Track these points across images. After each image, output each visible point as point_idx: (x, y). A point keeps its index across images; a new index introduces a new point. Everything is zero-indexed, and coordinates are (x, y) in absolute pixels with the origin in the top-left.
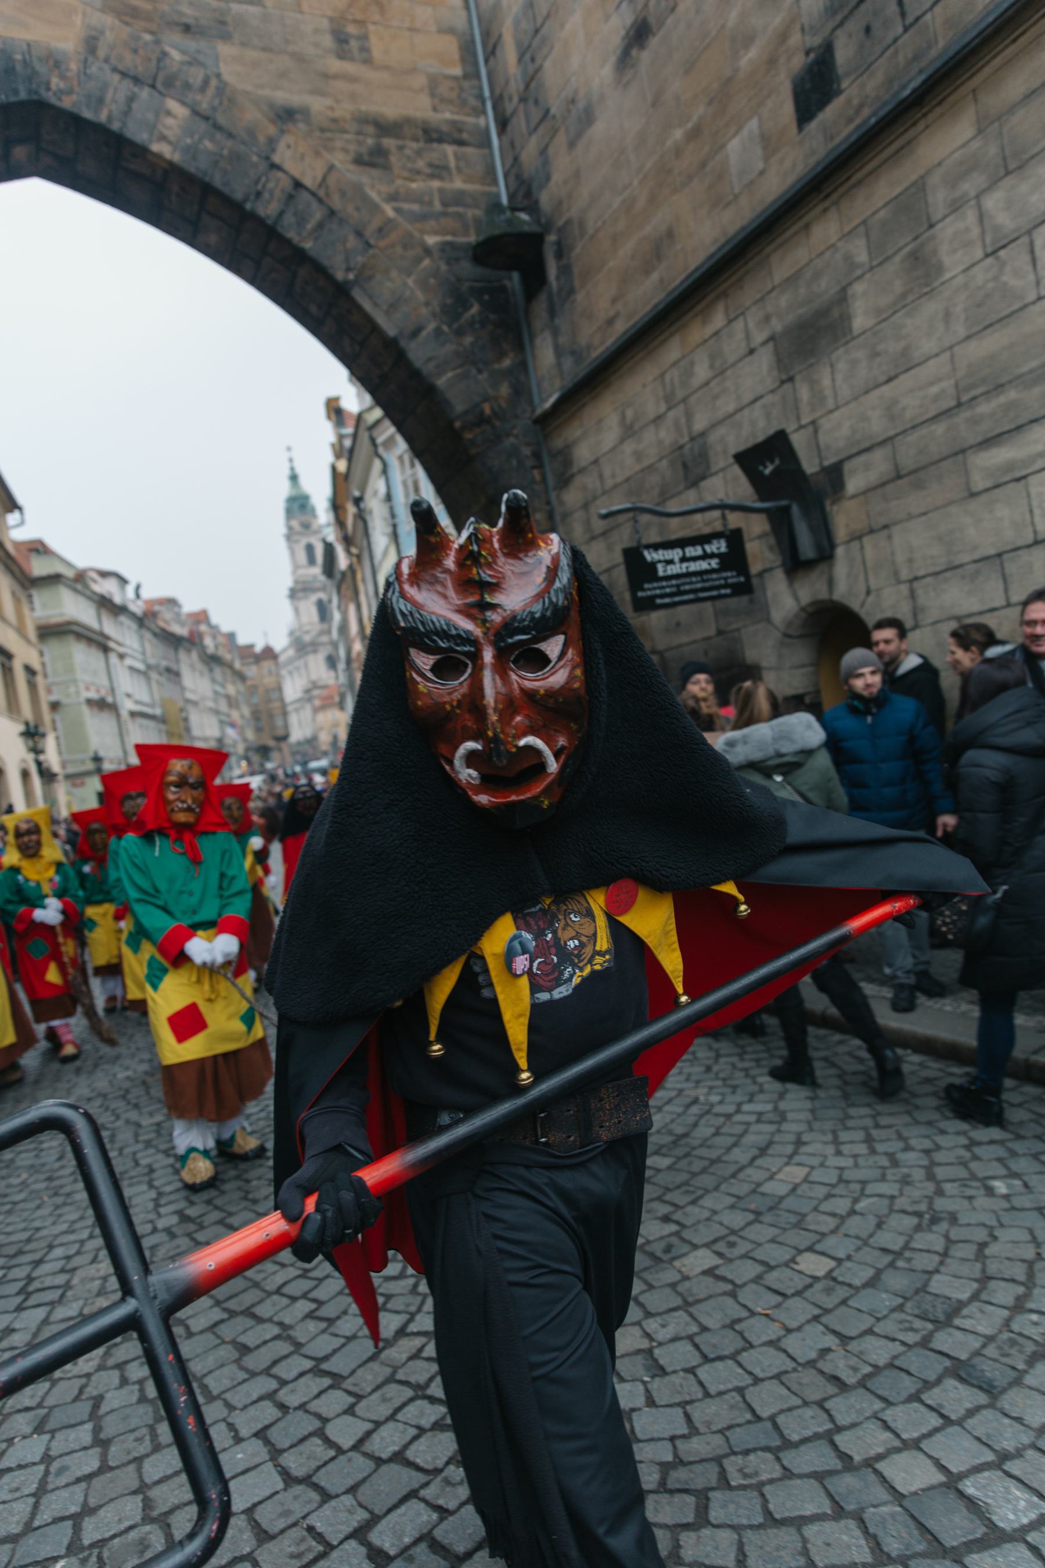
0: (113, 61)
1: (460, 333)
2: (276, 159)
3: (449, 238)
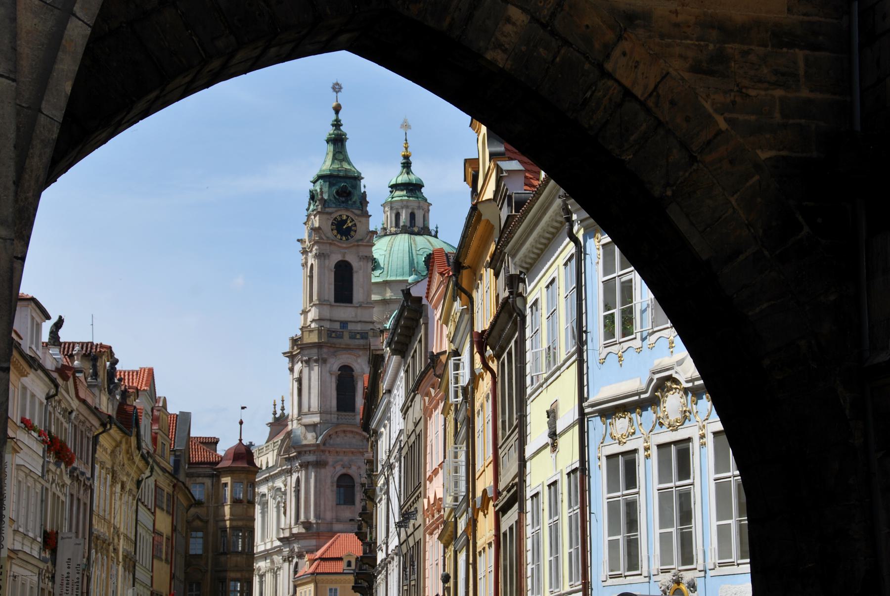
2: (609, 67)
3: (784, 153)
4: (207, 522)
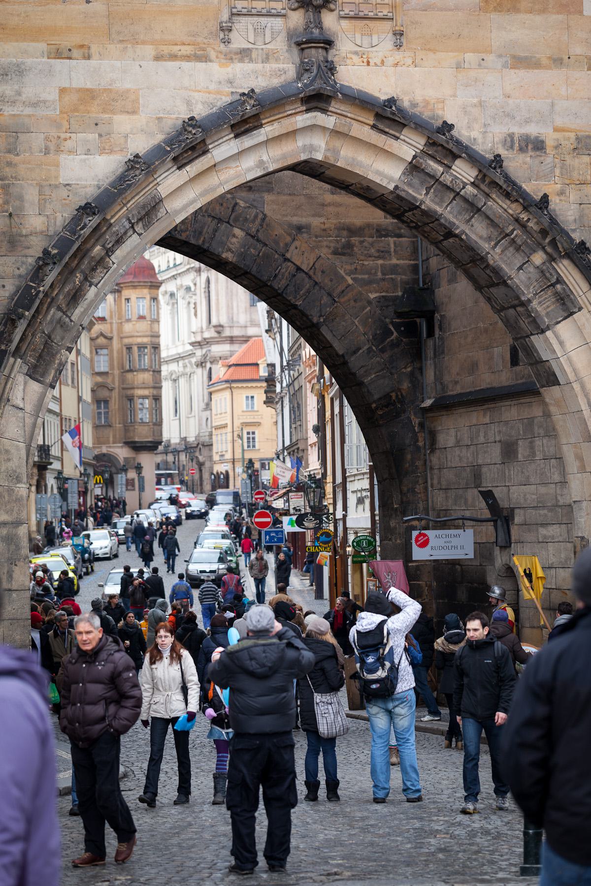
0: (210, 211)
1: (383, 351)
2: (288, 255)
4: (111, 339)
